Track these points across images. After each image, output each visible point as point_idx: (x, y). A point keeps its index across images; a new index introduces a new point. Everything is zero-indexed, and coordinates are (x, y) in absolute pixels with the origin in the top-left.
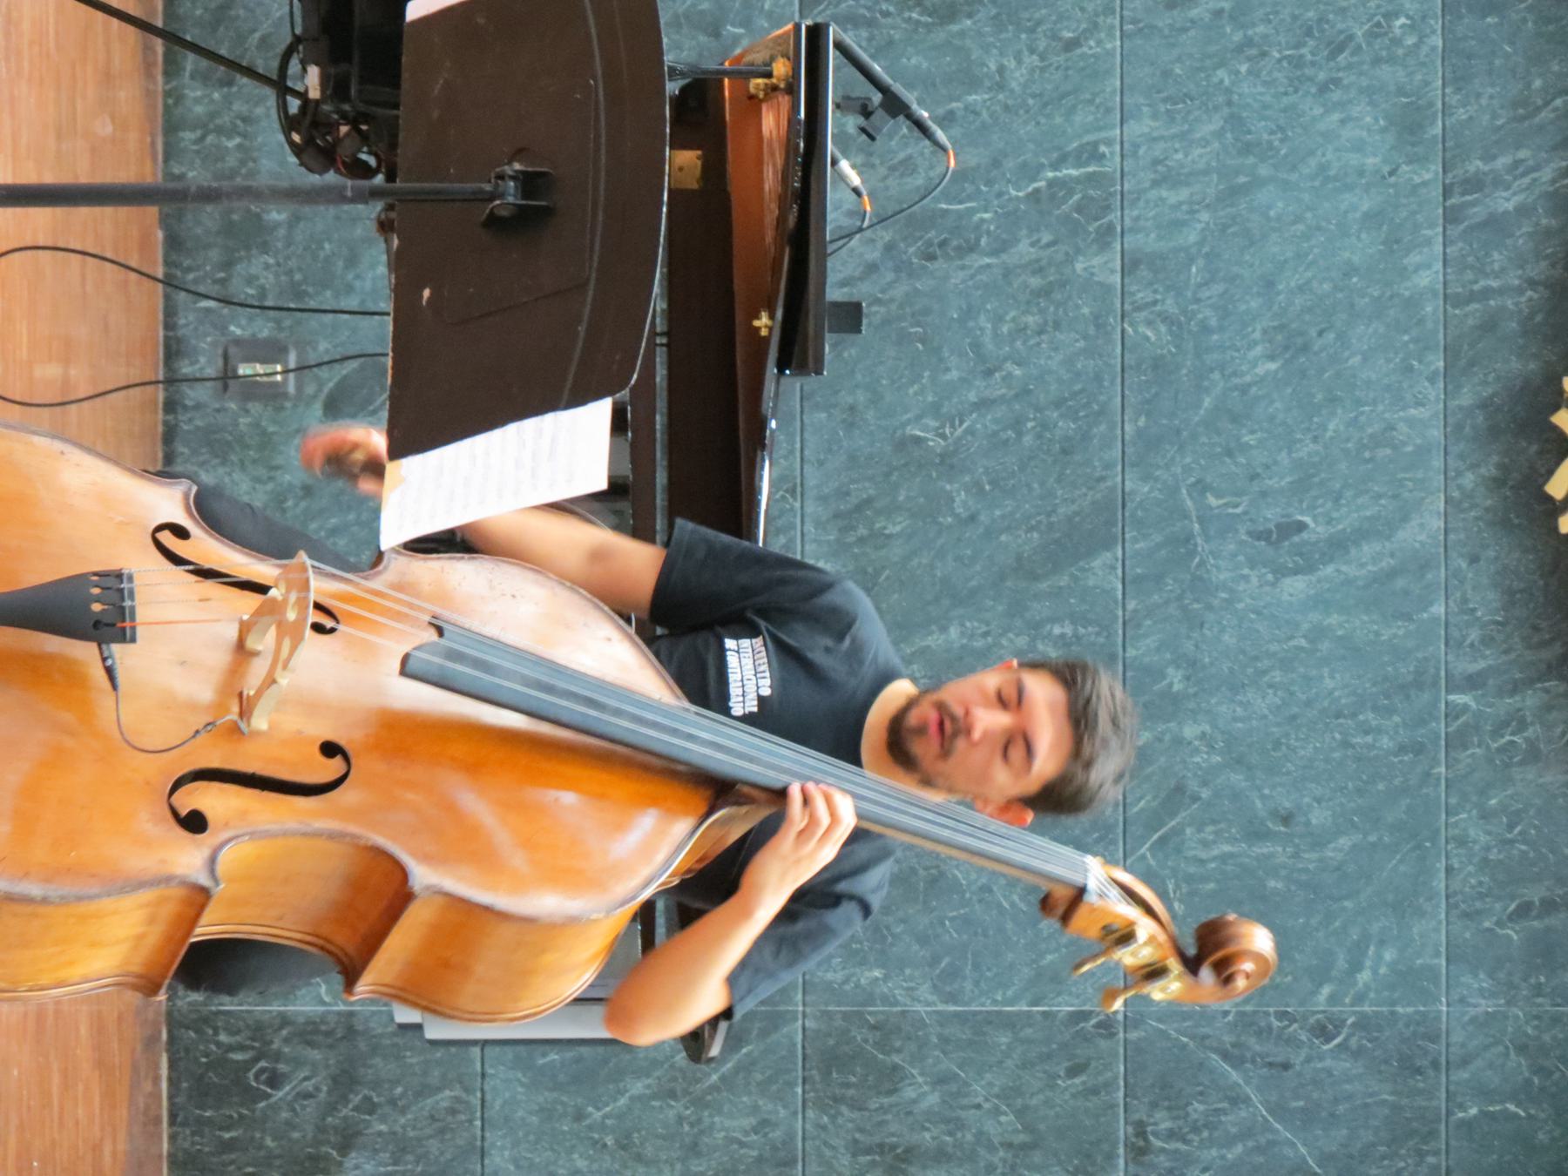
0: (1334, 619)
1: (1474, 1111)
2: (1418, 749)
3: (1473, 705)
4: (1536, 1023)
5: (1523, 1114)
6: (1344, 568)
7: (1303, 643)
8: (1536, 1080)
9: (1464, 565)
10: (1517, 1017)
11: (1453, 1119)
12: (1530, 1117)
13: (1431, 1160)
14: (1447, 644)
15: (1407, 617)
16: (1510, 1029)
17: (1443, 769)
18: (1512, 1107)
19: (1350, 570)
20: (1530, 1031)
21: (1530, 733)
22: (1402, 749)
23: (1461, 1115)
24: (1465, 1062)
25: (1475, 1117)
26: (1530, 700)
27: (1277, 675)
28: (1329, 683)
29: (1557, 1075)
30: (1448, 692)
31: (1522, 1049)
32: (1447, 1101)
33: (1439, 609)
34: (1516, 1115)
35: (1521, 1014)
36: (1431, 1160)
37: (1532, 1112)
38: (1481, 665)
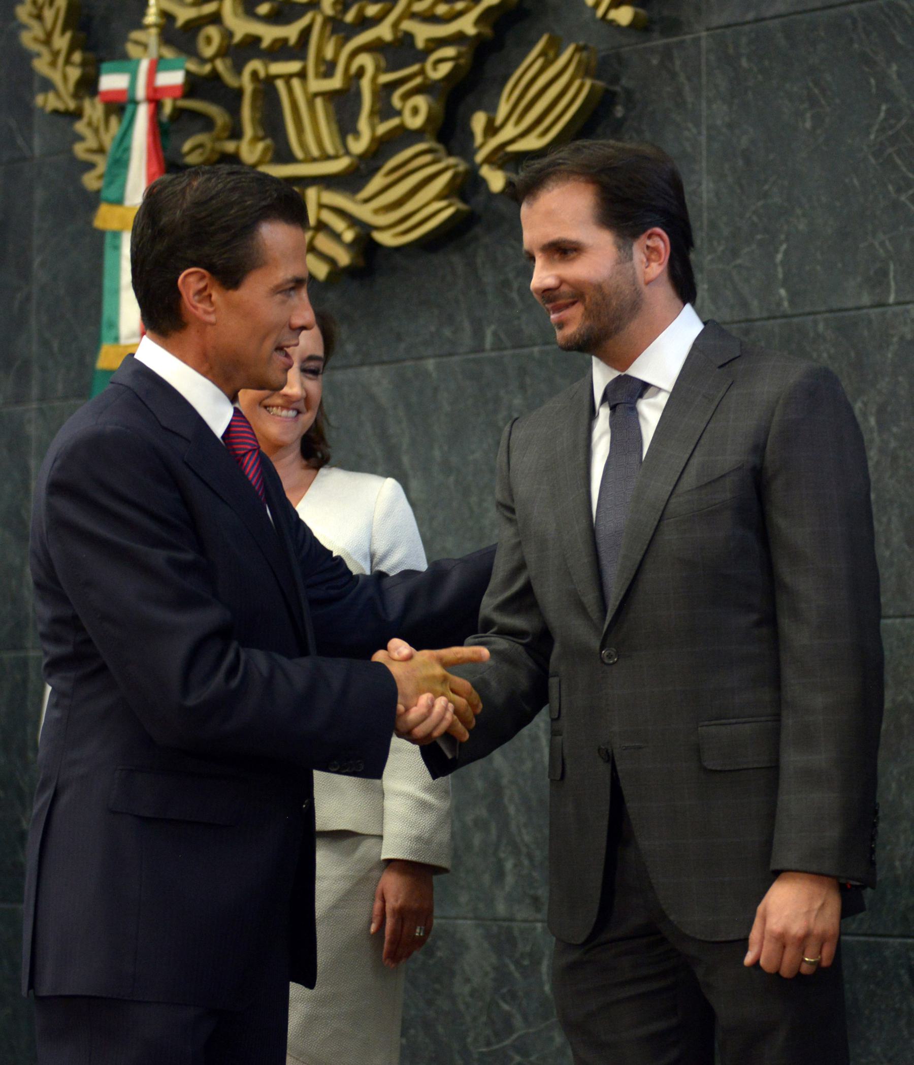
0: (437, 453)
1: (783, 292)
2: (522, 371)
3: (493, 327)
4: (715, 243)
5: (784, 246)
6: (405, 447)
7: (452, 479)
8: (759, 237)
9: (402, 346)
10: (712, 260)
11: (789, 311)
12: (787, 239)
13: (821, 327)
14: (451, 354)
15: (436, 389)
16: (721, 266)
17: (536, 350)
18: (779, 257)
19: (406, 441)
20: (721, 248)
21: (511, 276)
22: (523, 387)
23: (786, 304)
24: (744, 305)
25: (788, 291)
26: (489, 278)
27: (474, 499)
28: (478, 455)
29: (755, 219)
30: (483, 350)
31: (735, 253)
32: (775, 318)
33: (430, 364)
34: (786, 253)
35: (709, 257)
36: (821, 327)
37: (782, 237)
38: (467, 325)
